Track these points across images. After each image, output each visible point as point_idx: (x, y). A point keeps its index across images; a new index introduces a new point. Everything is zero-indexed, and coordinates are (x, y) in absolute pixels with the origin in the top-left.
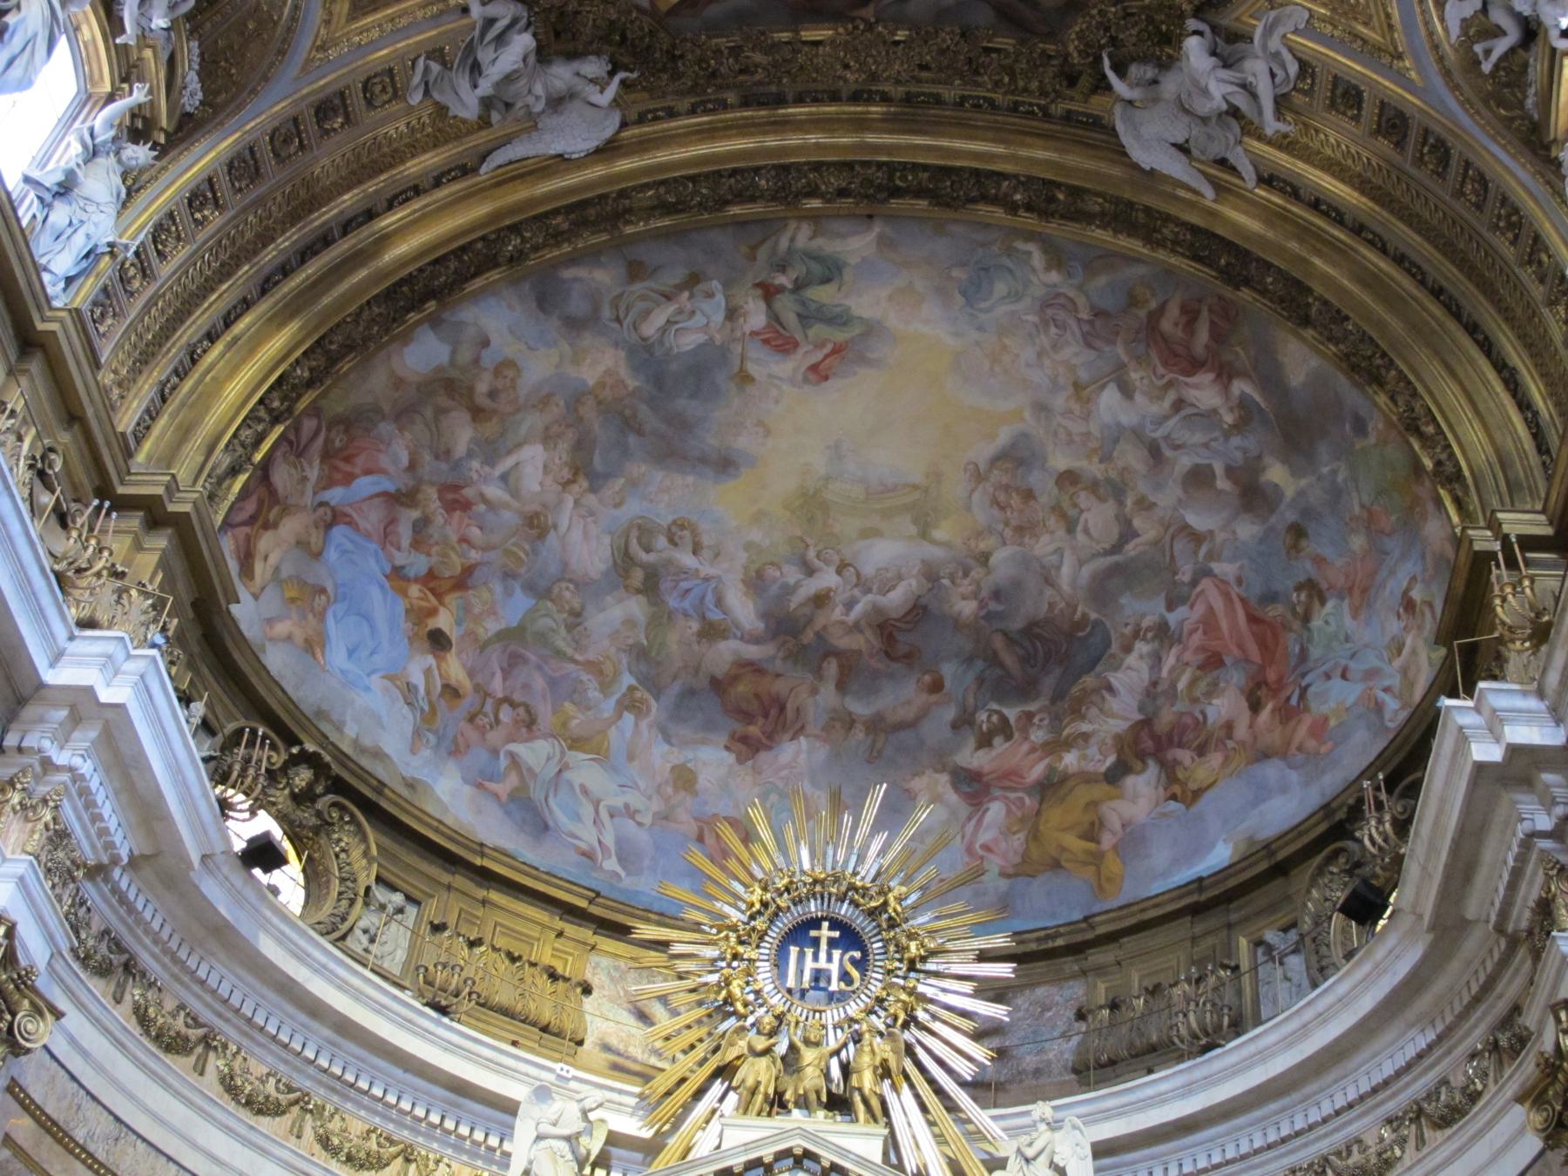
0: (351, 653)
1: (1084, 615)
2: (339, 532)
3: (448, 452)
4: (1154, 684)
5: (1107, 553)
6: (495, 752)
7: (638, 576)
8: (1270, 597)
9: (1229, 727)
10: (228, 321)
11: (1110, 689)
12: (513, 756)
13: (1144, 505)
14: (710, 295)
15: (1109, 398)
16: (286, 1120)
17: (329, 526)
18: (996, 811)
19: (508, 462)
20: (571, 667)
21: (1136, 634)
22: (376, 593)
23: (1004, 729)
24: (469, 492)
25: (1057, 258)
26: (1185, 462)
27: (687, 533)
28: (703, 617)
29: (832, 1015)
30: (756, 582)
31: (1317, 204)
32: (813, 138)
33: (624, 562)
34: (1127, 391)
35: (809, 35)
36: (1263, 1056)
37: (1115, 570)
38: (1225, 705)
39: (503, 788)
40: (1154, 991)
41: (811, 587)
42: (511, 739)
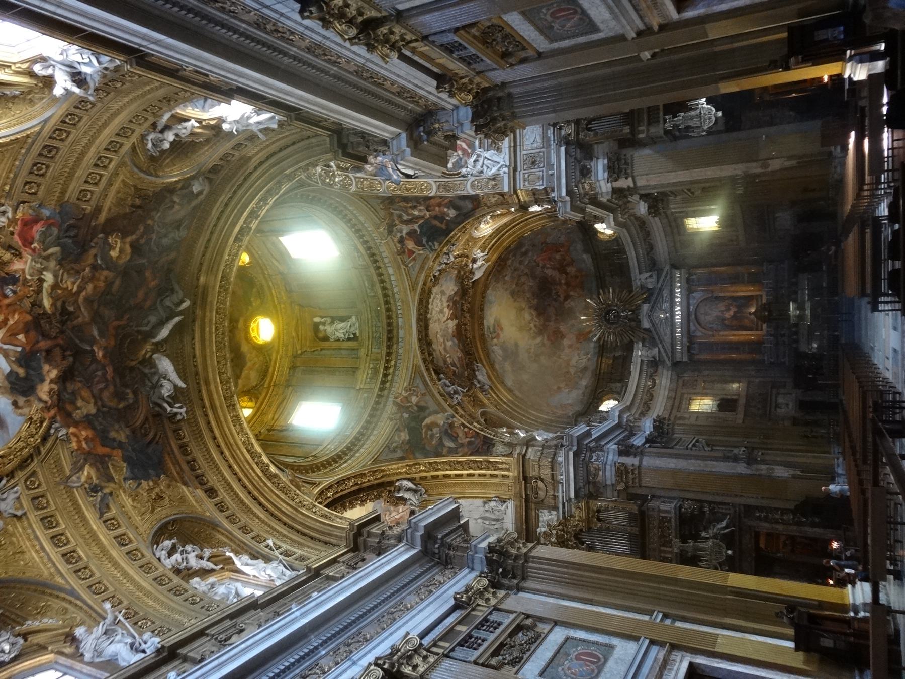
15: (506, 278)
18: (572, 293)
30: (534, 338)
38: (558, 256)
39: (581, 375)
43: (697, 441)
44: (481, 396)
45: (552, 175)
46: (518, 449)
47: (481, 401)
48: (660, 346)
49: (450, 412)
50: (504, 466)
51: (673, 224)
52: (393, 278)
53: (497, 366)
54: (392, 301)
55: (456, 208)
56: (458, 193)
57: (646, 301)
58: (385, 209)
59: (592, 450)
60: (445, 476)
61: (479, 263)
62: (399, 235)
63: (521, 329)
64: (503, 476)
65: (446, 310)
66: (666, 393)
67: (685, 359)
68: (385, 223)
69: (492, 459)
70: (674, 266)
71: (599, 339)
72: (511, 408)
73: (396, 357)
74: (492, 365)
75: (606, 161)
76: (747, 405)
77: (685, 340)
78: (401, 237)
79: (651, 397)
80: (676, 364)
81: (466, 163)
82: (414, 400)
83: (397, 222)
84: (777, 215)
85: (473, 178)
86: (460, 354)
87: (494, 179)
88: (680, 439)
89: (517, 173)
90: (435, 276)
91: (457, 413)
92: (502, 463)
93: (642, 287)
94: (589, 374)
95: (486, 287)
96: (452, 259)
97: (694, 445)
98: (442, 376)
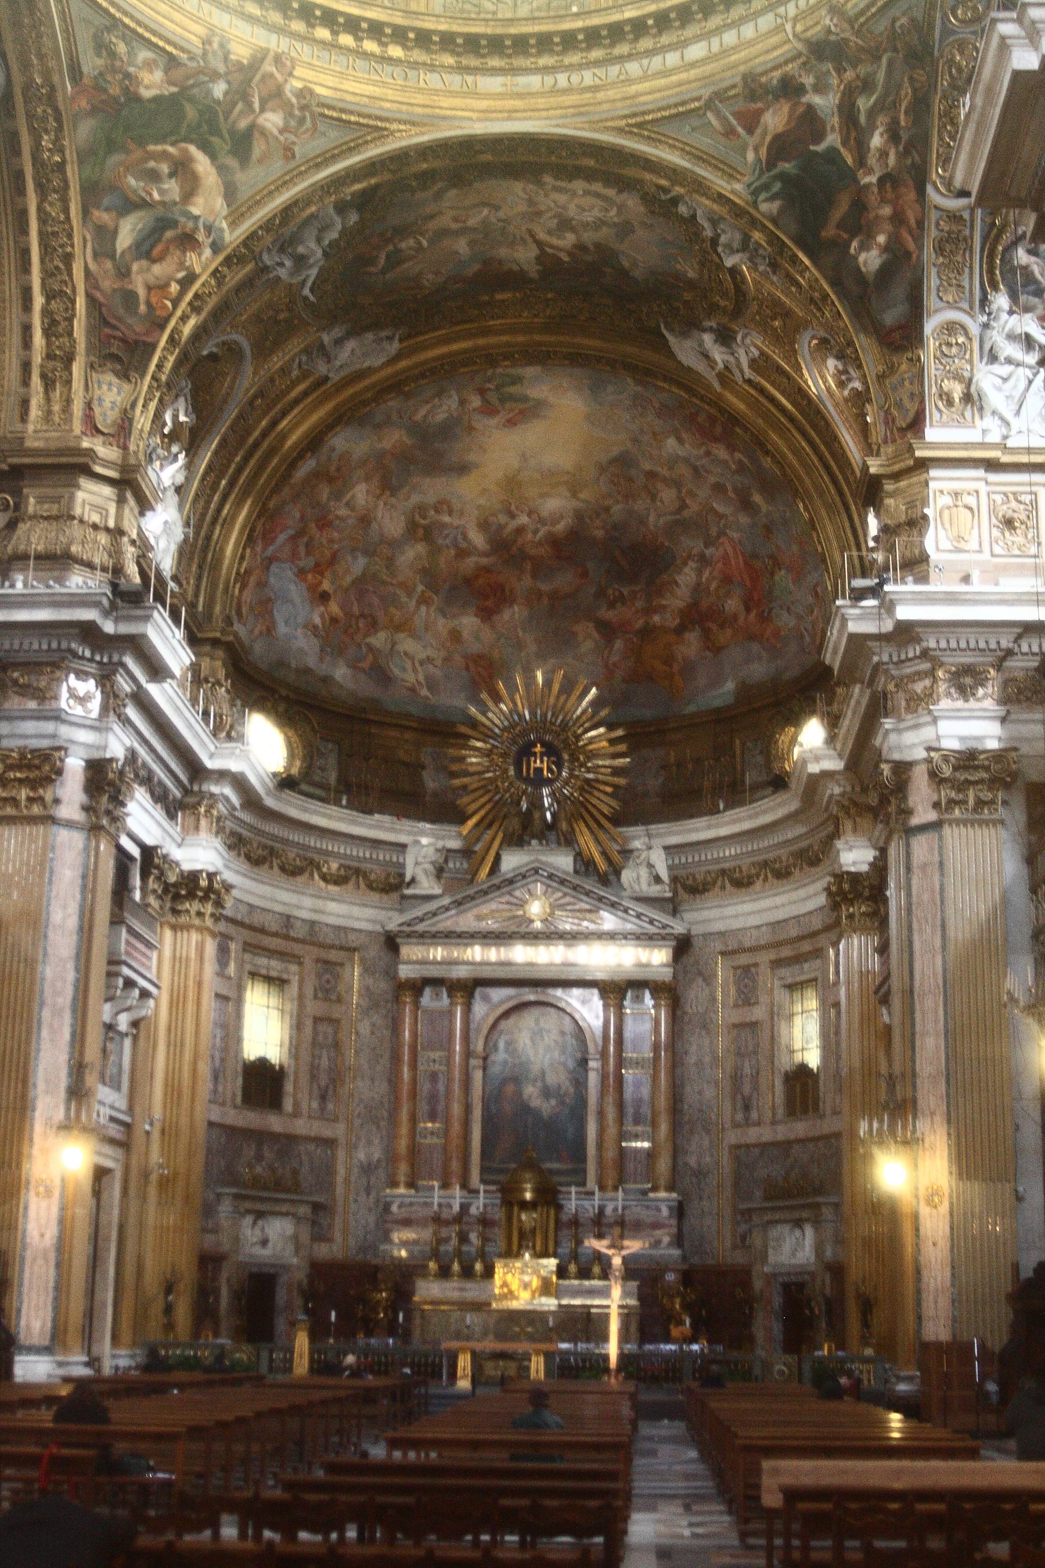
0: (286, 622)
1: (662, 544)
2: (274, 568)
3: (318, 504)
4: (698, 584)
5: (671, 514)
6: (359, 646)
7: (421, 531)
8: (755, 556)
9: (735, 617)
10: (219, 510)
11: (676, 583)
12: (368, 645)
13: (691, 494)
14: (450, 397)
15: (671, 442)
16: (307, 875)
17: (268, 569)
18: (619, 644)
19: (348, 496)
20: (391, 588)
21: (689, 557)
22: (293, 587)
23: (621, 599)
24: (331, 517)
25: (638, 382)
26: (712, 479)
27: (445, 507)
28: (456, 545)
29: (545, 791)
30: (484, 525)
31: (772, 400)
32: (505, 338)
33: (412, 527)
34: (680, 441)
35: (499, 296)
36: (739, 820)
37: (676, 522)
38: (733, 605)
39: (365, 665)
40: (698, 761)
41: (513, 524)
42: (366, 636)
43: (145, 994)
44: (295, 346)
45: (966, 579)
46: (107, 451)
47: (277, 344)
48: (446, 901)
49: (232, 236)
50: (56, 408)
51: (806, 947)
52: (672, 59)
53: (393, 403)
54: (596, 54)
55: (886, 273)
56: (932, 280)
57: (585, 865)
58: (893, 35)
59: (105, 679)
60: (23, 213)
61: (719, 355)
62: (808, 80)
63: (512, 483)
64: (25, 403)
65: (569, 240)
66: (305, 915)
67: (405, 972)
68: (846, 35)
69: (77, 369)
70: (682, 947)
71: (474, 724)
72: (256, 445)
73: (415, 65)
74: (395, 386)
75: (993, 745)
76: (260, 1137)
77: (461, 973)
78: (801, 90)
79: (291, 871)
80: (391, 943)
81: (1027, 309)
82: (272, 120)
83: (849, 75)
84: (809, 1231)
85: (974, 329)
86: (429, 280)
87: (967, 398)
88: (149, 945)
89: (980, 473)
90: (675, 201)
91: (228, 261)
92: (68, 402)
93: (627, 853)
94: (366, 688)
95: (643, 373)
96: (729, 262)
97: (129, 984)
98: (353, 218)
